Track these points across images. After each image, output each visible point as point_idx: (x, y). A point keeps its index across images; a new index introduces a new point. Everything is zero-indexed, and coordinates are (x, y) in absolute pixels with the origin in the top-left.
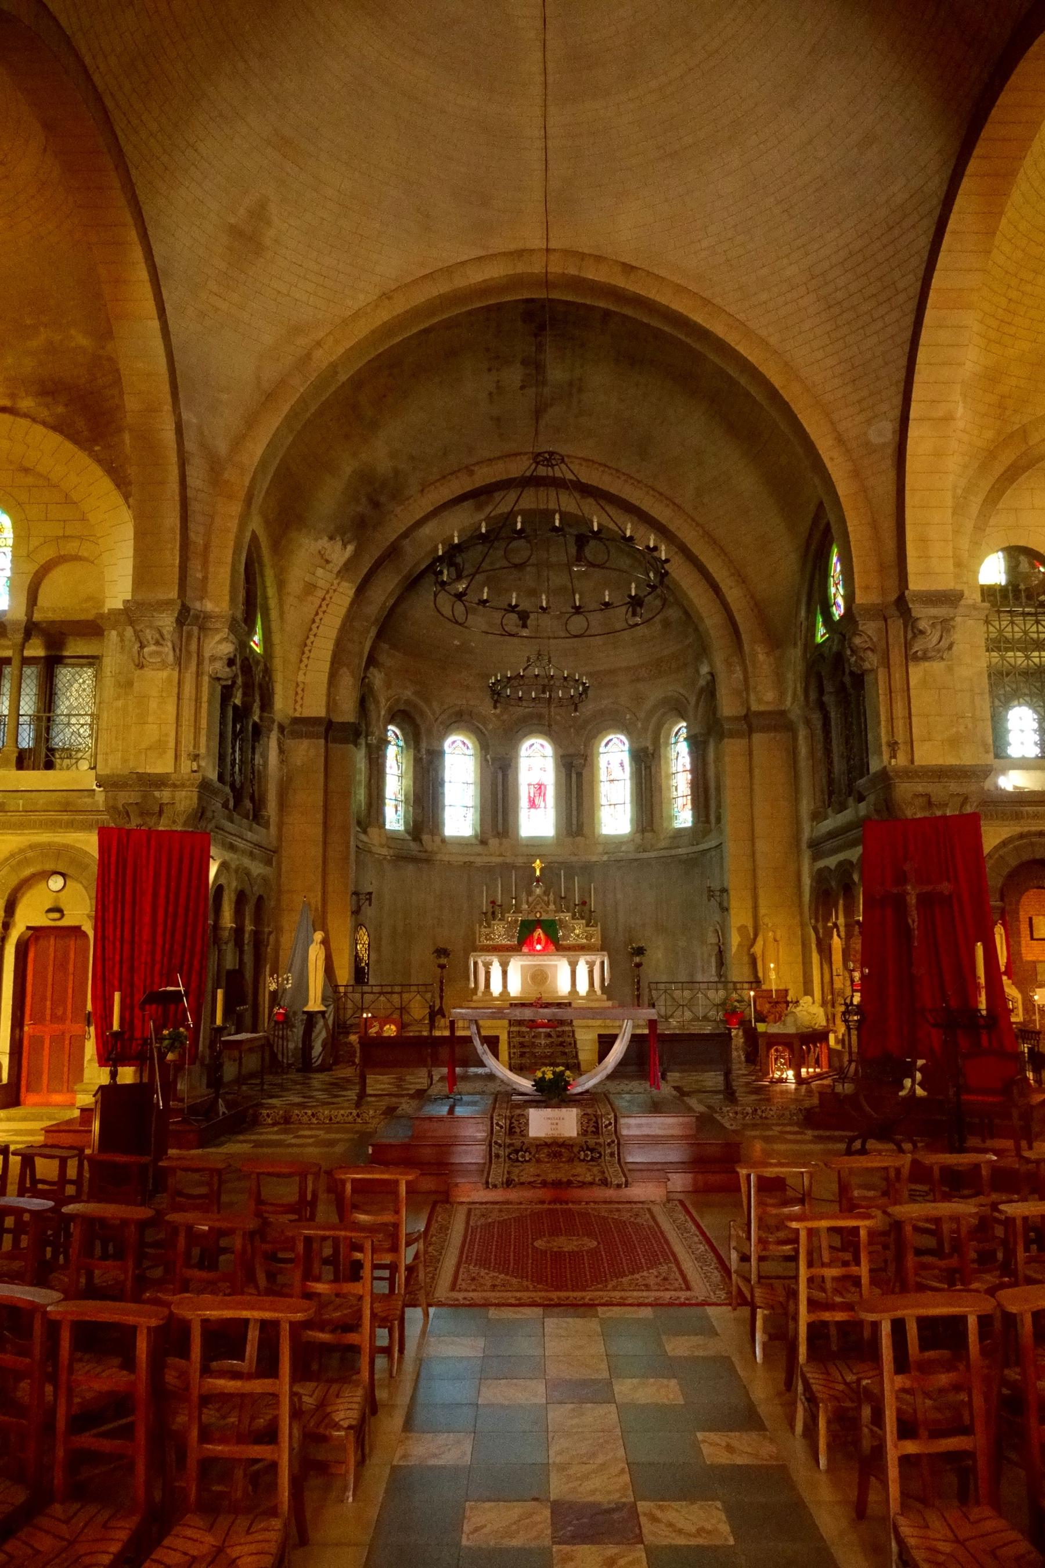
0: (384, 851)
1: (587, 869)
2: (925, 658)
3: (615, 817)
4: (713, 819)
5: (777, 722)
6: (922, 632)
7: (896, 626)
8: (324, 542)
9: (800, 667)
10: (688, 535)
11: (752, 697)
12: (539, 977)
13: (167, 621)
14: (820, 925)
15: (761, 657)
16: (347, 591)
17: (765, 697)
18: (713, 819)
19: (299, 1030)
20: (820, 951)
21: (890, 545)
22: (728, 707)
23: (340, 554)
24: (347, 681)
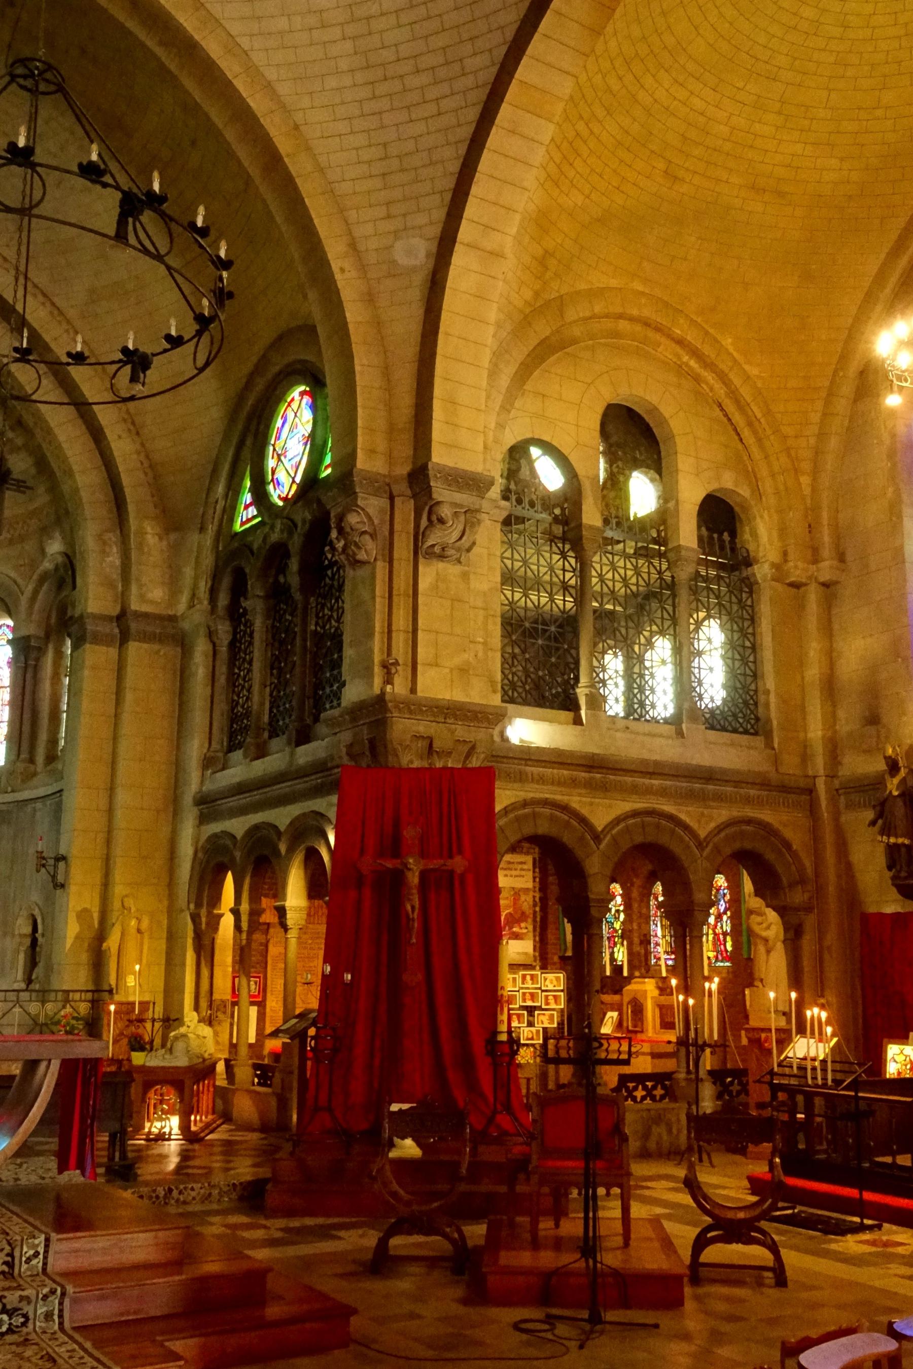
2: (442, 557)
4: (40, 758)
6: (441, 521)
7: (405, 509)
9: (208, 561)
11: (134, 589)
14: (203, 912)
15: (151, 539)
17: (151, 595)
18: (40, 758)
20: (199, 947)
22: (95, 599)
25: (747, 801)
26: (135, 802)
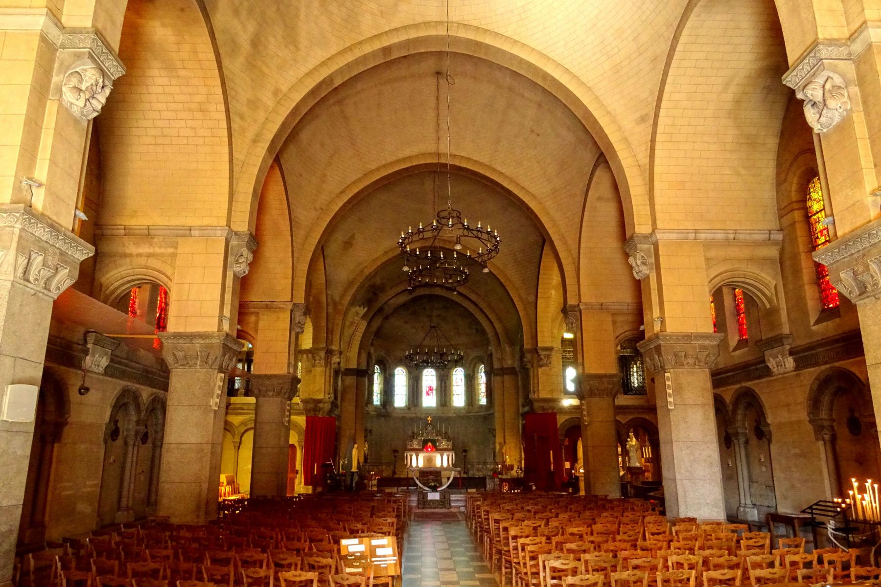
0: (373, 413)
1: (448, 419)
3: (459, 399)
5: (511, 371)
7: (536, 356)
8: (358, 308)
10: (483, 305)
12: (429, 460)
13: (322, 354)
15: (507, 349)
16: (364, 323)
17: (508, 363)
19: (349, 478)
21: (534, 330)
22: (496, 365)
23: (362, 311)
24: (364, 356)
25: (639, 413)
26: (509, 415)
